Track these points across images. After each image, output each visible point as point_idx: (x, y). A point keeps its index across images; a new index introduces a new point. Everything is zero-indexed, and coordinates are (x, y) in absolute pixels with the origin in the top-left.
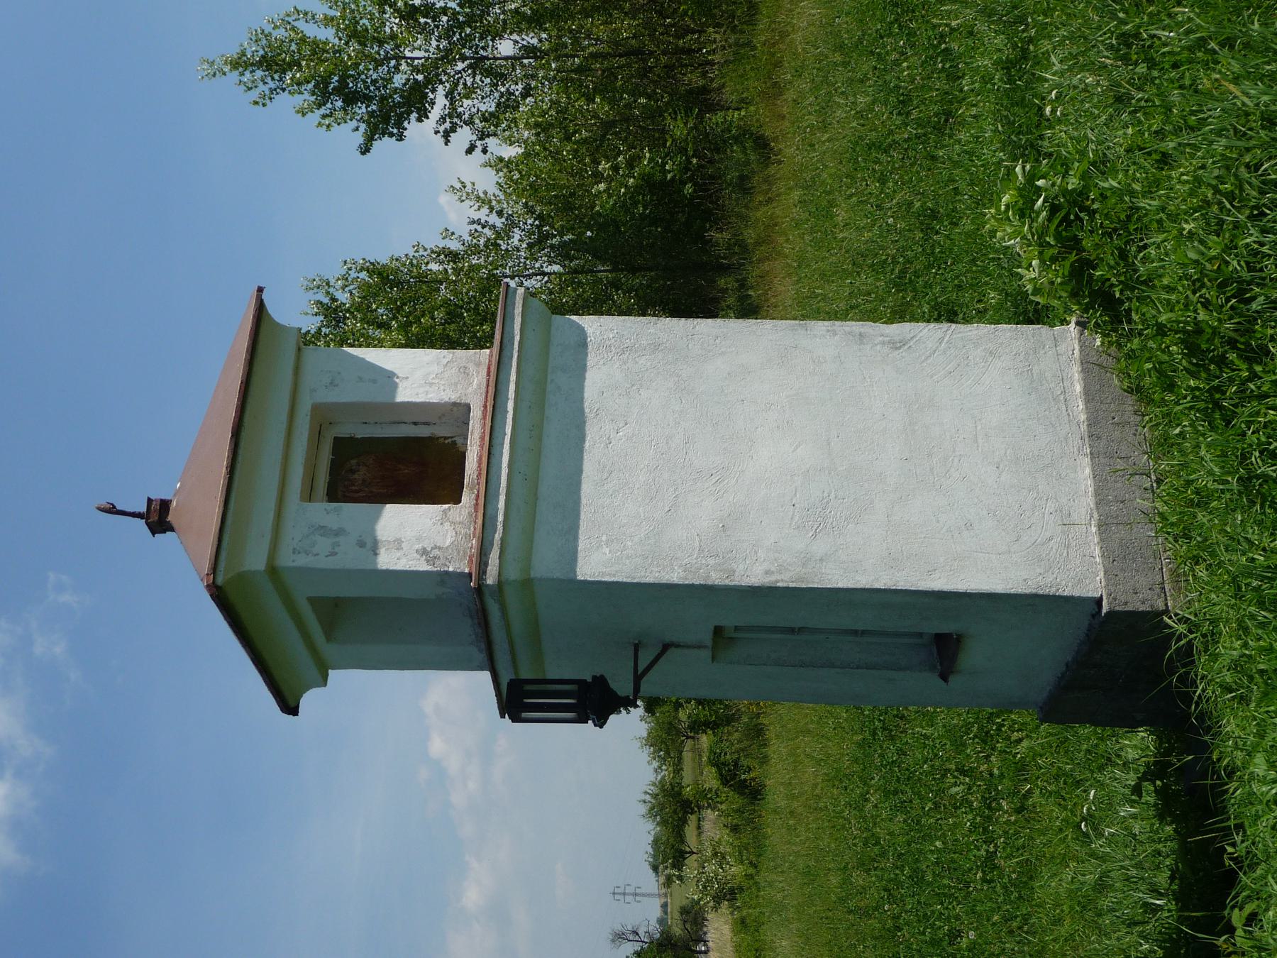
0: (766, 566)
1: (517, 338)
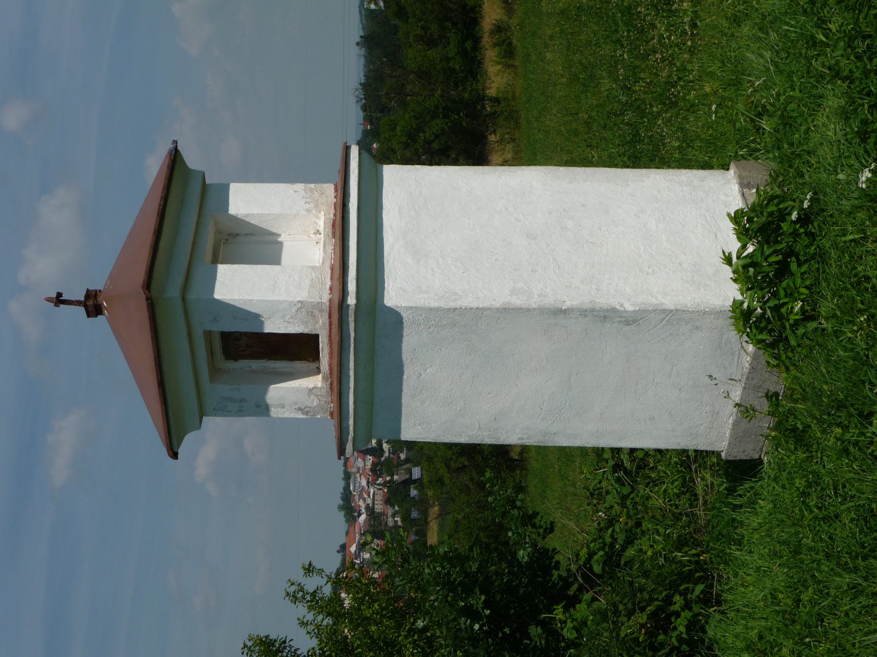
0: (520, 436)
1: (352, 335)
